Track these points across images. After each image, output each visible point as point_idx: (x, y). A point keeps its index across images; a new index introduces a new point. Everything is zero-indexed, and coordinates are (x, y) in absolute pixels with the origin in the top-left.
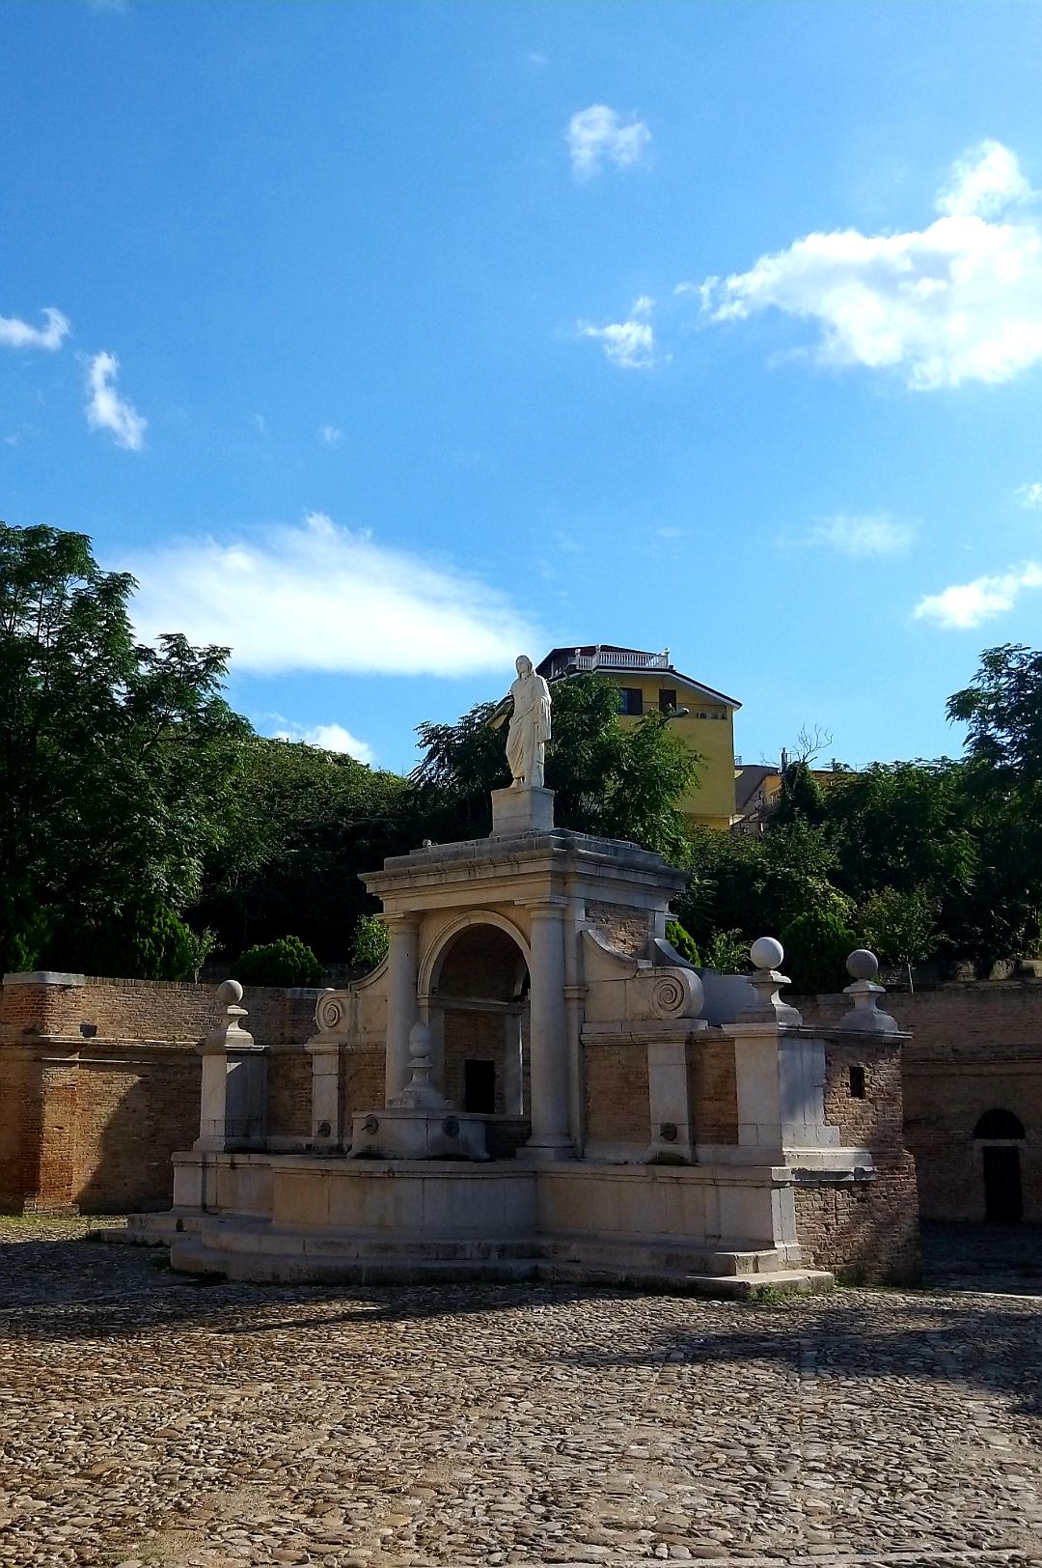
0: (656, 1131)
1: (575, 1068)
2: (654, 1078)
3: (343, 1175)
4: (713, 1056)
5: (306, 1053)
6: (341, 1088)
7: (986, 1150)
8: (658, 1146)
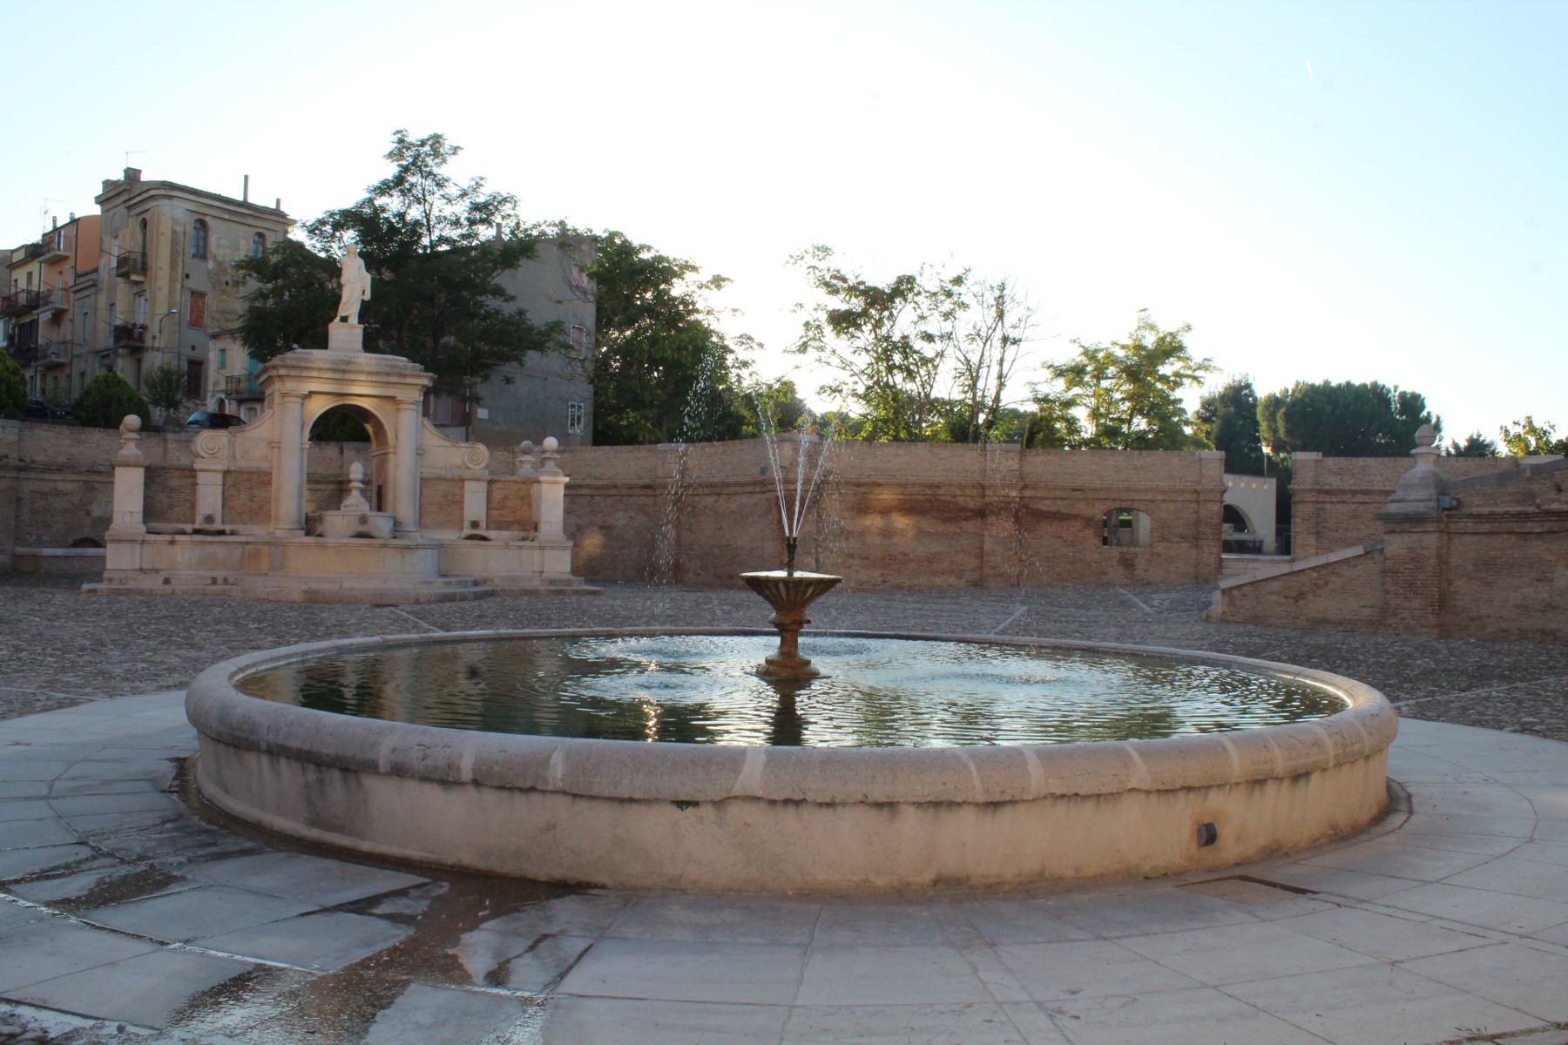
0: (466, 523)
1: (418, 491)
2: (468, 498)
4: (499, 489)
5: (194, 471)
6: (223, 493)
8: (468, 531)
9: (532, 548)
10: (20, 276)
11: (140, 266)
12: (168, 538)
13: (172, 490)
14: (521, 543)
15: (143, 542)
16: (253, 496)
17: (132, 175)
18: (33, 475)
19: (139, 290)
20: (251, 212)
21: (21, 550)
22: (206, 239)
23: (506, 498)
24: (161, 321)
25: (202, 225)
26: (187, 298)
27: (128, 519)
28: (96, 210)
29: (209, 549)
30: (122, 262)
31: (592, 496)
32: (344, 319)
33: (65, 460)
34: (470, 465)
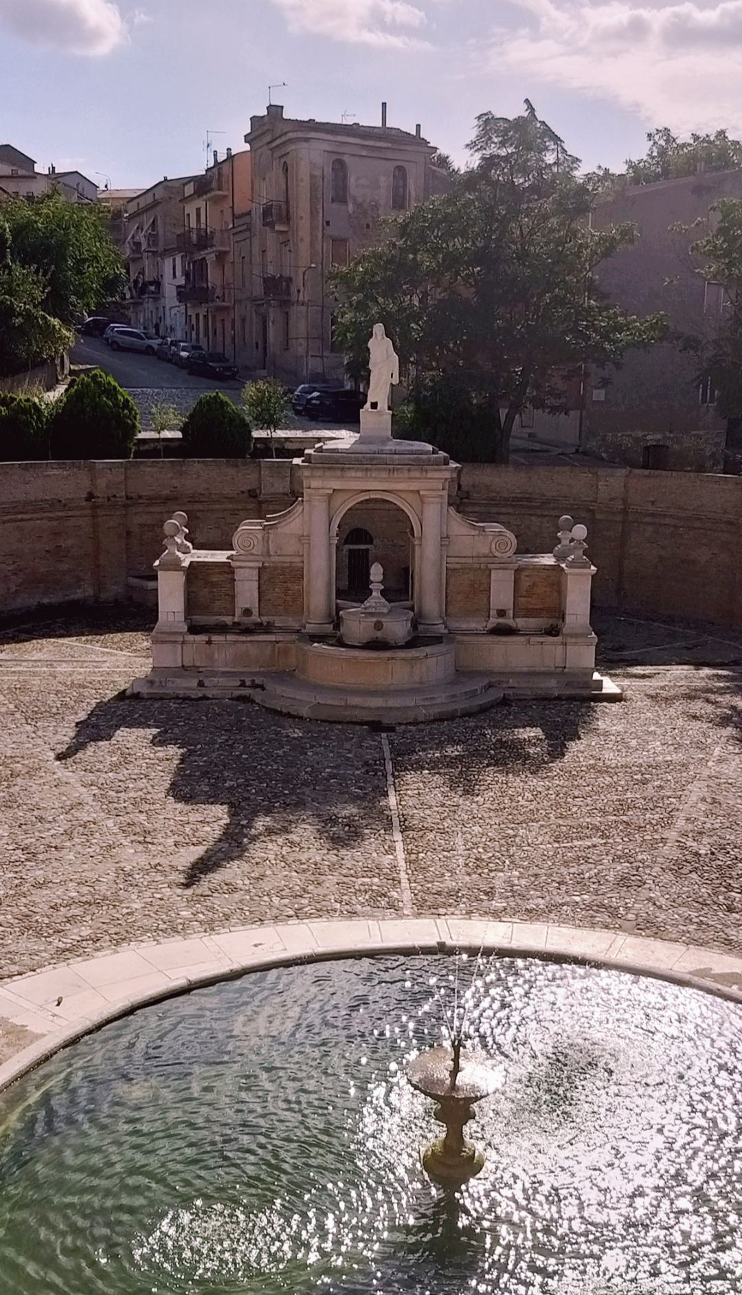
1: (444, 582)
3: (403, 659)
6: (259, 588)
7: (350, 550)
8: (494, 621)
9: (553, 644)
10: (190, 209)
11: (284, 213)
12: (204, 638)
13: (213, 585)
14: (541, 639)
15: (183, 642)
16: (287, 589)
17: (275, 111)
18: (140, 510)
19: (285, 241)
20: (390, 145)
21: (134, 581)
22: (345, 178)
23: (534, 584)
24: (304, 274)
25: (340, 166)
26: (328, 246)
27: (171, 618)
28: (247, 147)
29: (243, 647)
30: (267, 212)
31: (675, 527)
32: (374, 405)
33: (168, 492)
34: (497, 554)
